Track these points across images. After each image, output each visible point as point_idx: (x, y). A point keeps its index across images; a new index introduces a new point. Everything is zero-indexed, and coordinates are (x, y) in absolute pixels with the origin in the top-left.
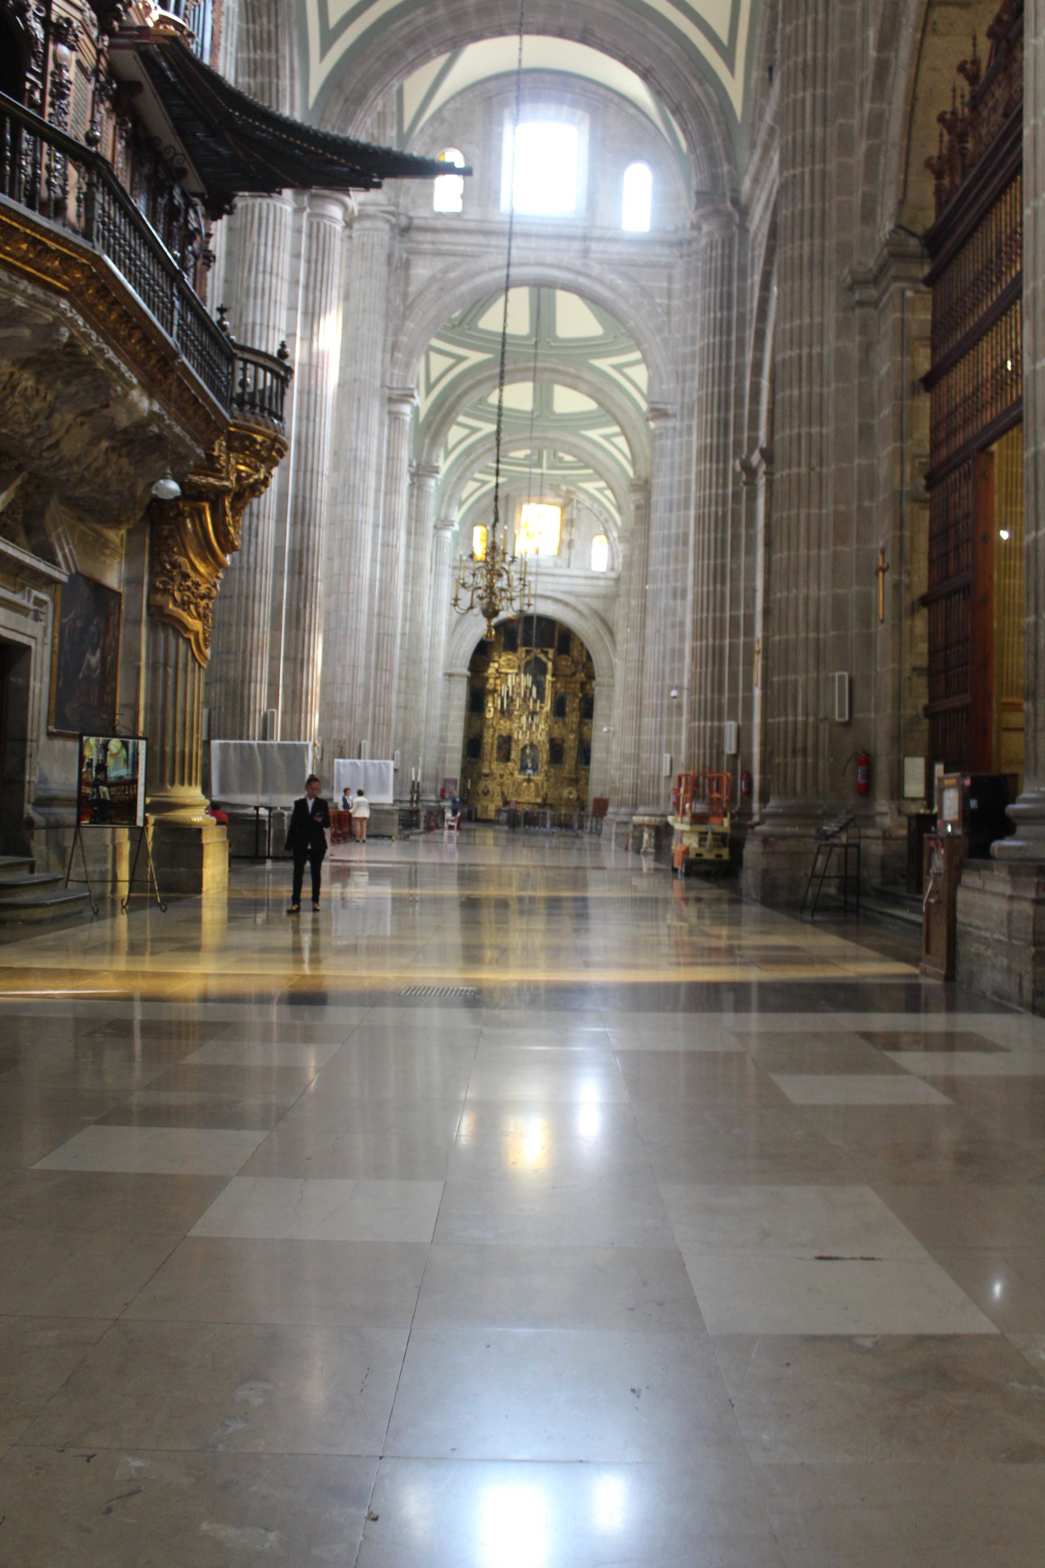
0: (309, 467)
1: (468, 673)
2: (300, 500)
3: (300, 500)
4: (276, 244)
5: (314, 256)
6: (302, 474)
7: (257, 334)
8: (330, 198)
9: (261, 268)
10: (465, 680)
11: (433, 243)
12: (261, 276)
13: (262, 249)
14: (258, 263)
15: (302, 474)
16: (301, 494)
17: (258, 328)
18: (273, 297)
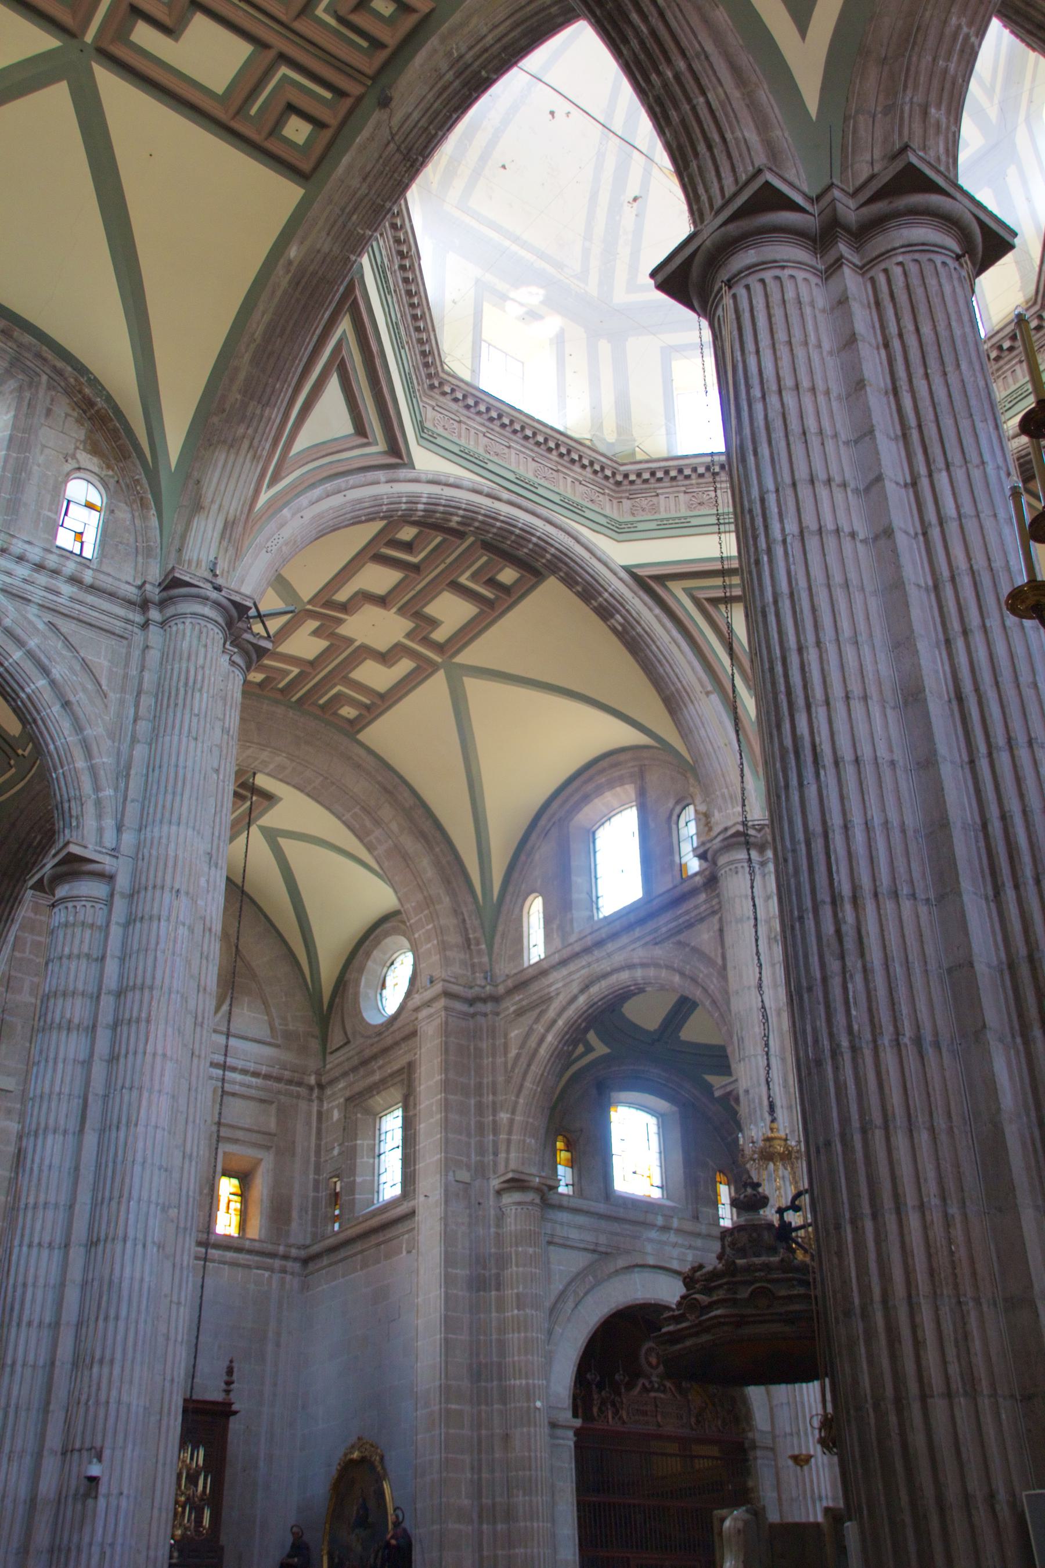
0: (1000, 740)
2: (996, 827)
3: (996, 827)
4: (781, 336)
5: (893, 329)
6: (983, 764)
7: (773, 509)
8: (897, 214)
9: (757, 392)
12: (759, 407)
13: (752, 361)
14: (748, 387)
15: (983, 764)
16: (994, 812)
17: (772, 498)
18: (794, 425)
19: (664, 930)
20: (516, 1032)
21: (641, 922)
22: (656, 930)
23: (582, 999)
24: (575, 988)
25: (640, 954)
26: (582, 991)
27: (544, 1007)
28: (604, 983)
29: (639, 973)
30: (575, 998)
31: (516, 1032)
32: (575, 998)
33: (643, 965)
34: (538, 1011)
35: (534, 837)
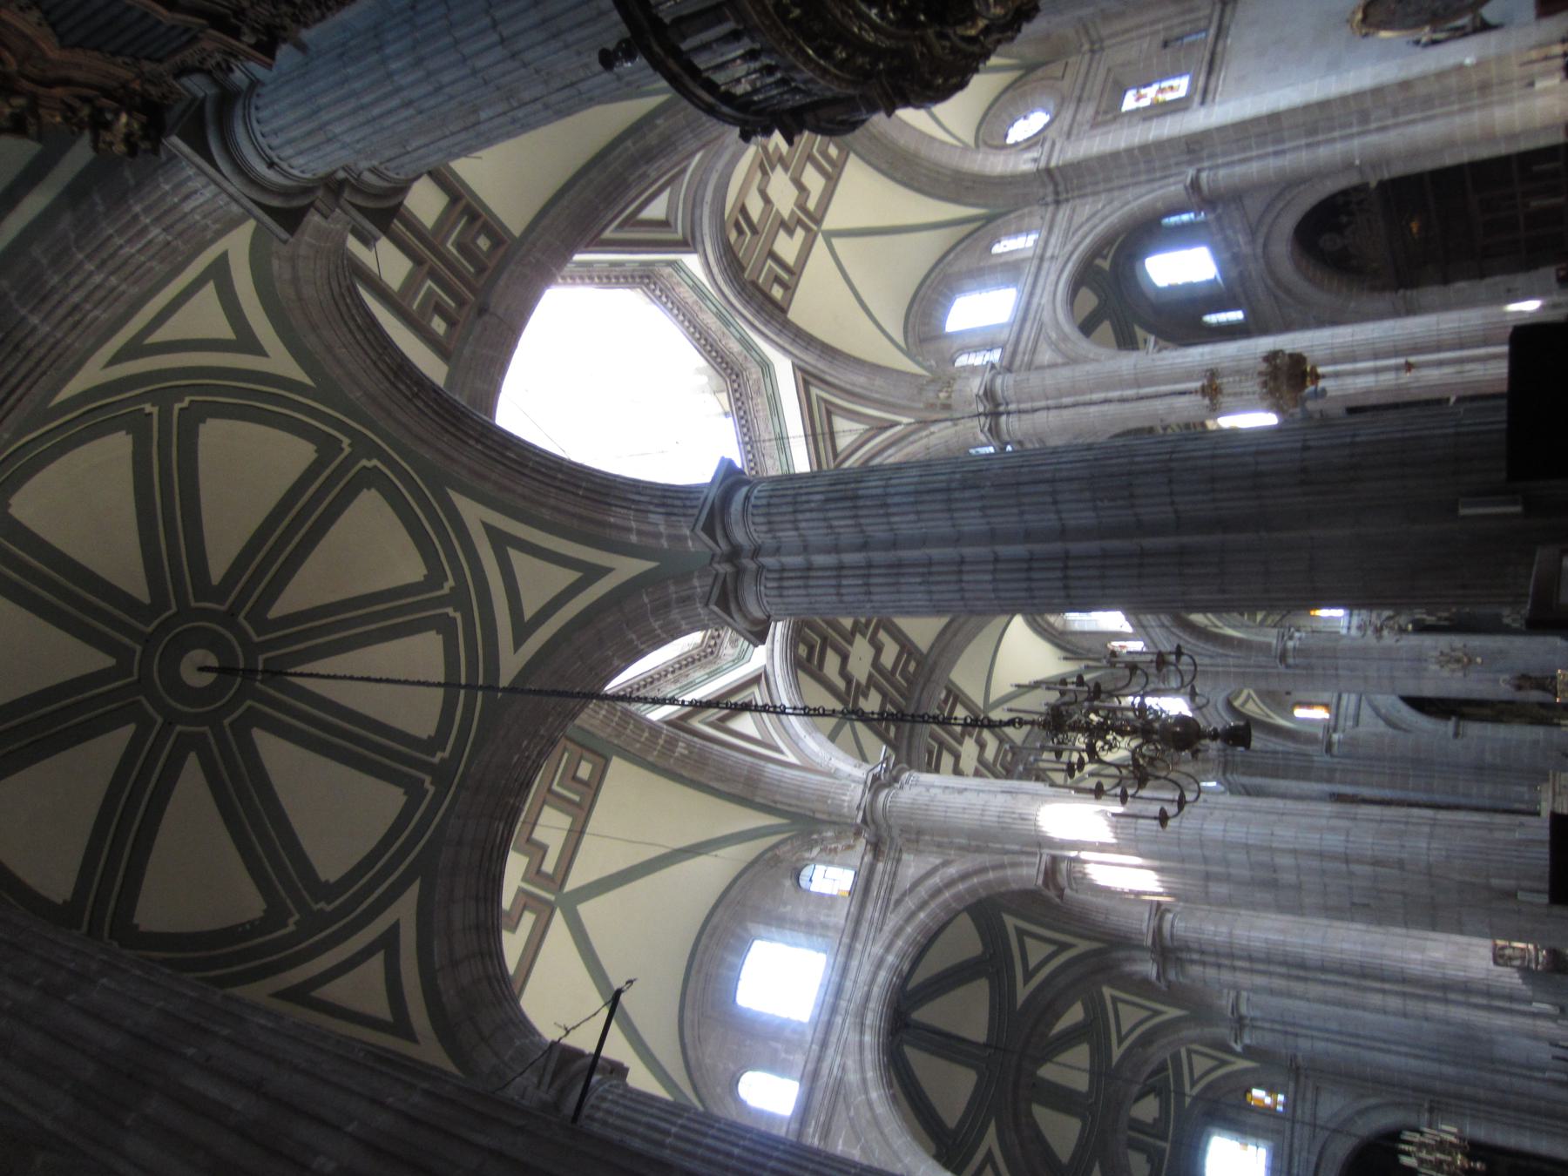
1: (1454, 719)
10: (1461, 723)
11: (1024, 354)
19: (877, 915)
20: (841, 1142)
21: (858, 922)
22: (871, 923)
23: (868, 1038)
24: (853, 1037)
25: (877, 950)
26: (862, 1033)
27: (843, 1092)
28: (872, 1005)
29: (890, 959)
30: (861, 1044)
31: (841, 1142)
32: (861, 1044)
33: (888, 949)
34: (841, 1099)
35: (690, 1053)
